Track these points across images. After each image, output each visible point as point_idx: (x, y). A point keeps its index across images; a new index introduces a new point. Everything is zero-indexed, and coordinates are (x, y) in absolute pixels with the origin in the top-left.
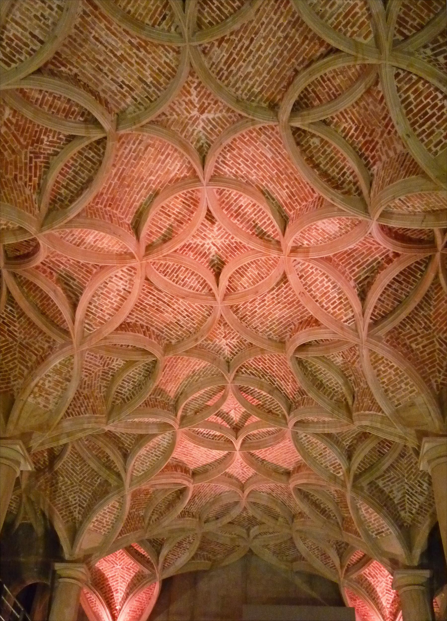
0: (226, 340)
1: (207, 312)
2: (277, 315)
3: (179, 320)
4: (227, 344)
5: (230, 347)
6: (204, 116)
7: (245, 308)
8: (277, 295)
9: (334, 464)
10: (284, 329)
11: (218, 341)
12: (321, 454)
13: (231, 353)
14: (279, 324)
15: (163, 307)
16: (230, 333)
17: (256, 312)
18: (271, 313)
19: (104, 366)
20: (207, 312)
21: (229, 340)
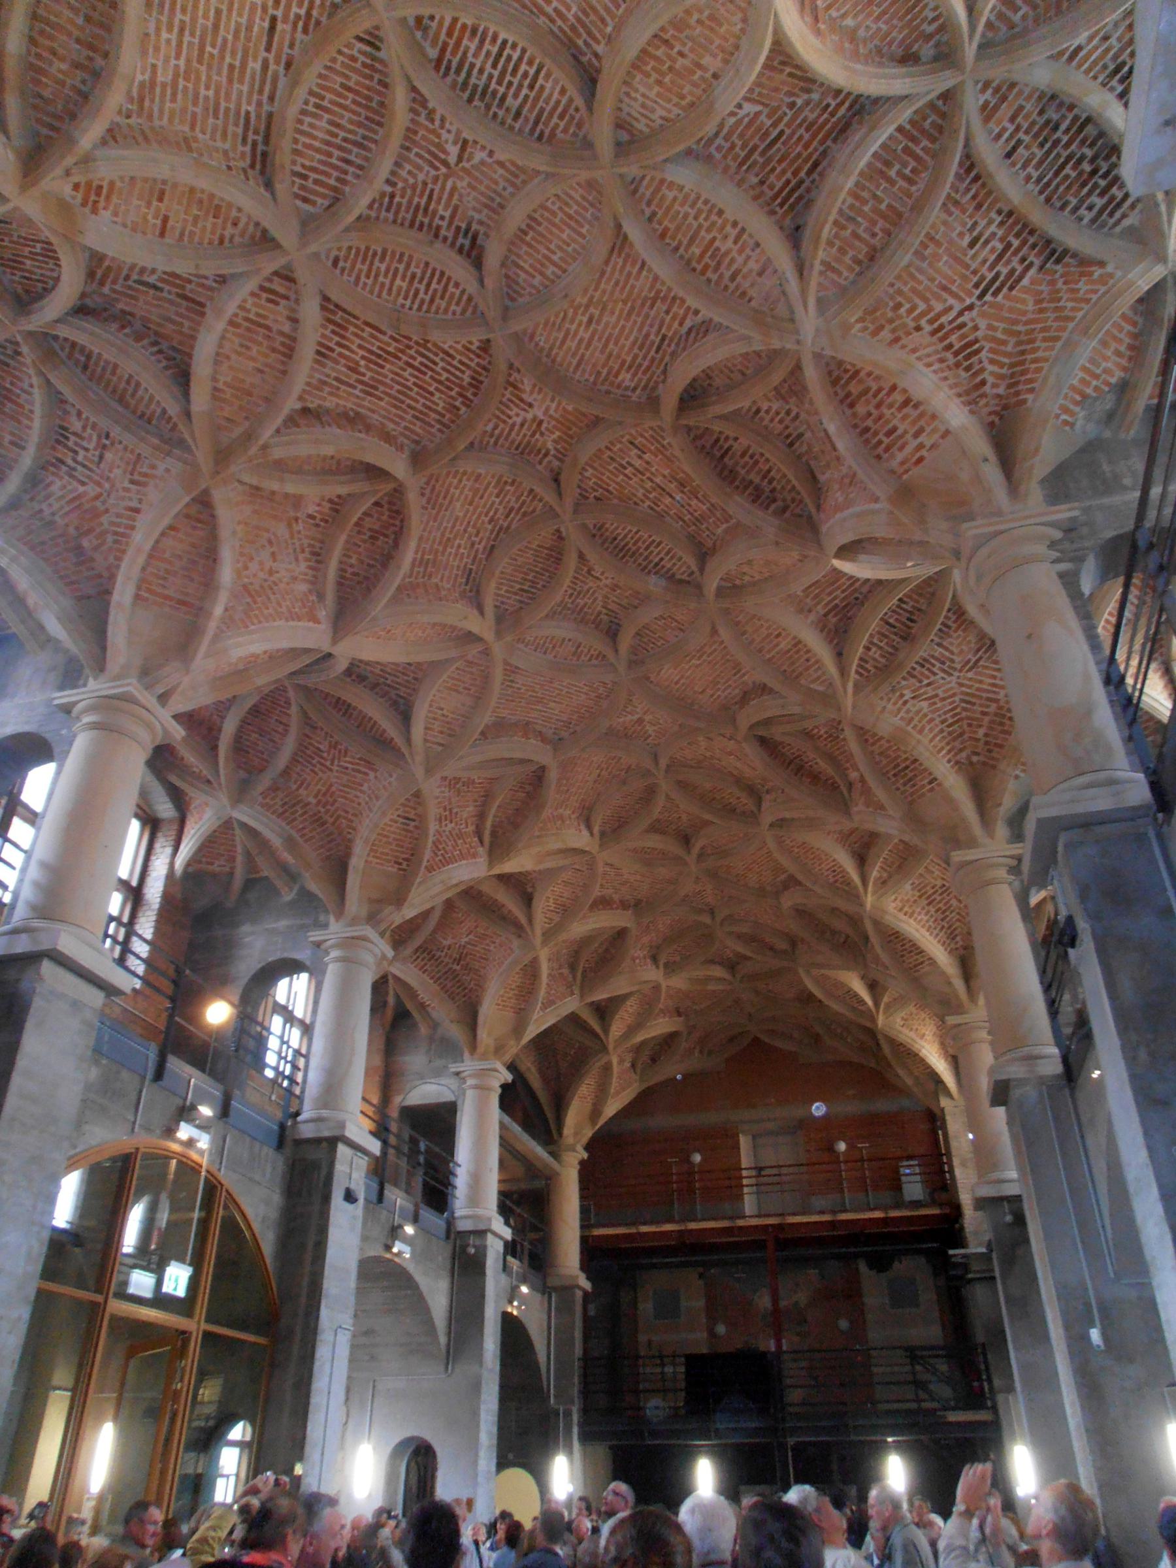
0: (534, 419)
1: (587, 474)
2: (458, 505)
3: (640, 457)
4: (530, 405)
5: (522, 400)
6: (636, 717)
7: (518, 499)
8: (473, 545)
9: (108, 198)
10: (434, 487)
11: (552, 412)
12: (160, 200)
13: (515, 387)
14: (448, 491)
15: (671, 487)
16: (533, 435)
17: (497, 496)
18: (470, 504)
19: (797, 416)
20: (587, 474)
21: (529, 416)
